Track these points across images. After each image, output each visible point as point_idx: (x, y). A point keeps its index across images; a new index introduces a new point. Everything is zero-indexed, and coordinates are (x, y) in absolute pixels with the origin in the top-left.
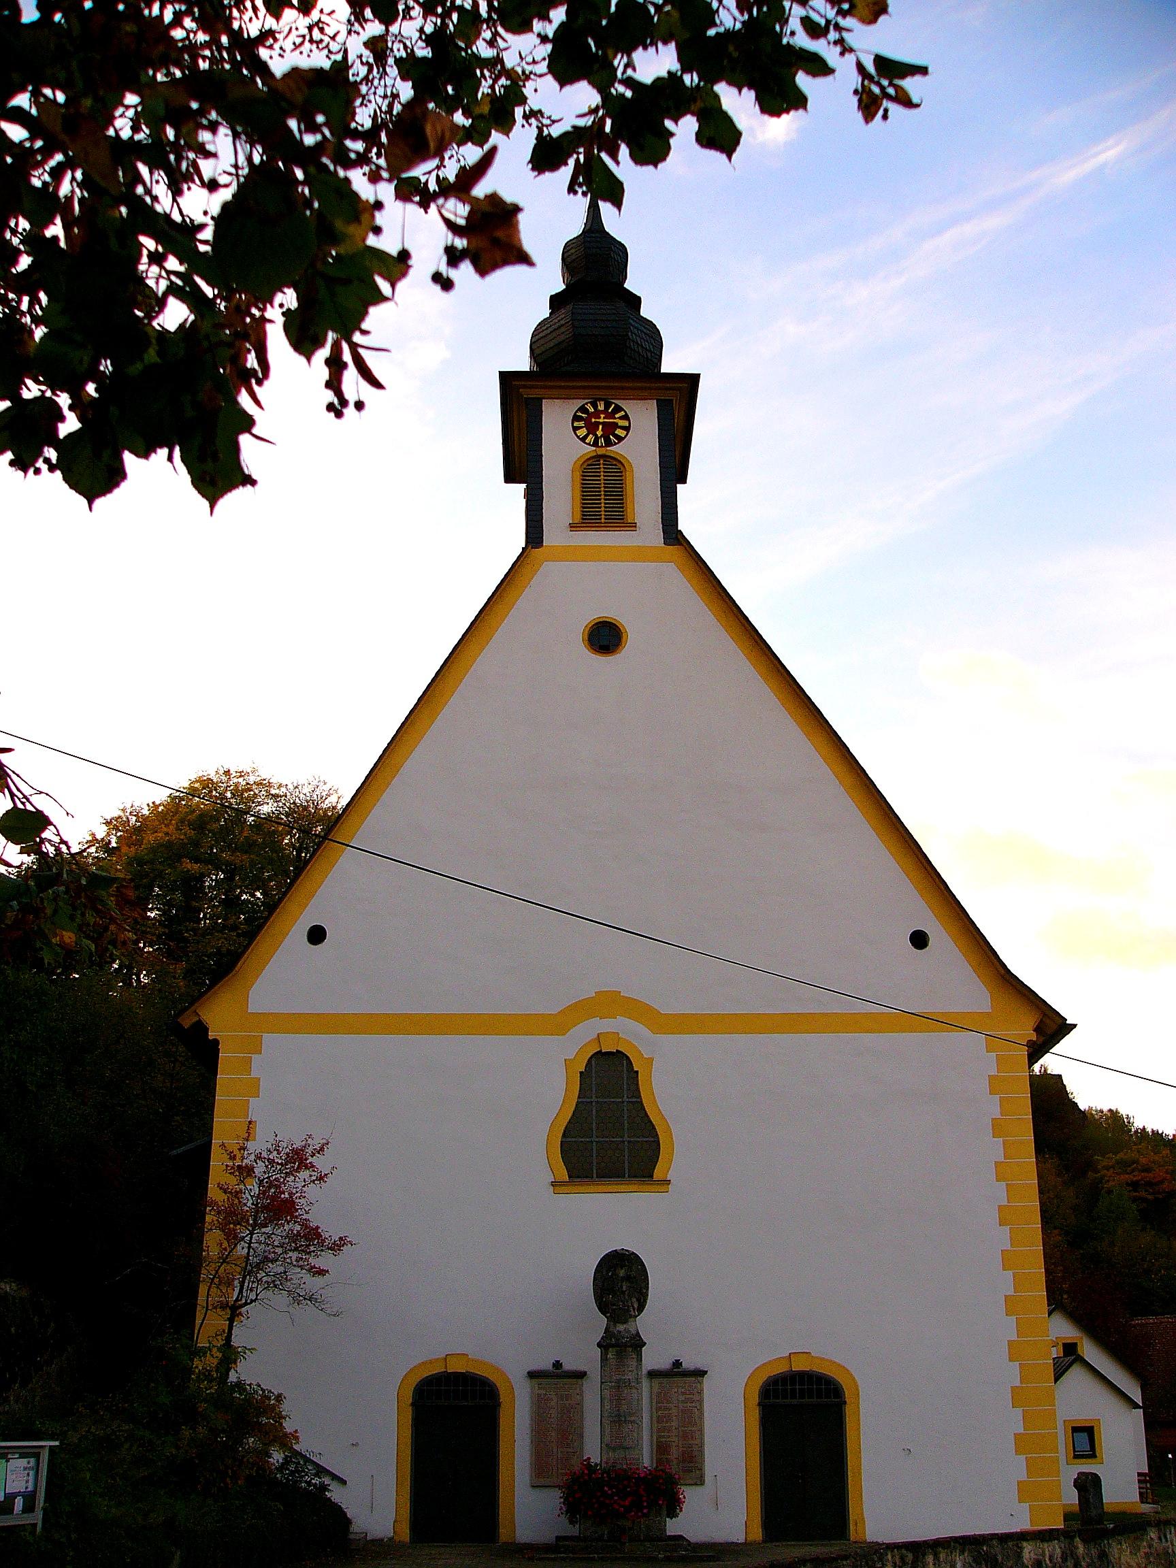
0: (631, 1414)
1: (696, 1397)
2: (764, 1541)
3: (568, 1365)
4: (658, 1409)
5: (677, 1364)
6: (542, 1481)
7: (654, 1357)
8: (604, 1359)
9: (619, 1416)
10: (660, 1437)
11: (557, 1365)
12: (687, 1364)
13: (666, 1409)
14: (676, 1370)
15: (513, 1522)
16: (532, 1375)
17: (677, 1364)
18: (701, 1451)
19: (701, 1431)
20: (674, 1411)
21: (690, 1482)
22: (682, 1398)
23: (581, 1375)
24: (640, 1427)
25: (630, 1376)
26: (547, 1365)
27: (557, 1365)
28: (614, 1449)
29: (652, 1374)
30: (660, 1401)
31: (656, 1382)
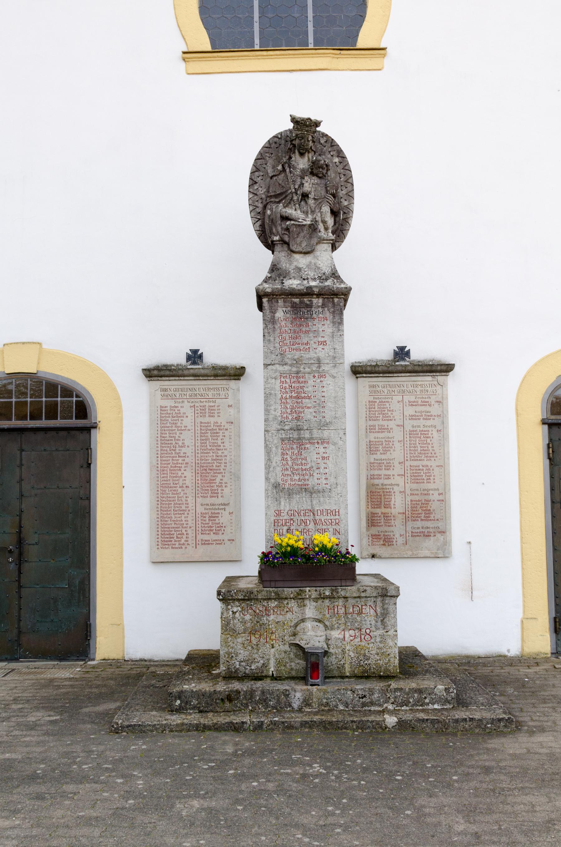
0: (323, 425)
1: (435, 410)
2: (556, 653)
3: (213, 357)
4: (371, 429)
5: (402, 353)
6: (168, 554)
7: (365, 334)
8: (270, 323)
9: (299, 429)
10: (372, 477)
11: (195, 356)
13: (382, 429)
14: (401, 364)
15: (119, 625)
16: (153, 373)
17: (402, 353)
18: (444, 501)
19: (444, 467)
20: (397, 434)
21: (426, 553)
22: (410, 411)
23: (237, 373)
24: (341, 450)
25: (322, 353)
26: (177, 357)
27: (195, 356)
28: (290, 493)
29: (358, 371)
30: (375, 412)
31: (365, 382)
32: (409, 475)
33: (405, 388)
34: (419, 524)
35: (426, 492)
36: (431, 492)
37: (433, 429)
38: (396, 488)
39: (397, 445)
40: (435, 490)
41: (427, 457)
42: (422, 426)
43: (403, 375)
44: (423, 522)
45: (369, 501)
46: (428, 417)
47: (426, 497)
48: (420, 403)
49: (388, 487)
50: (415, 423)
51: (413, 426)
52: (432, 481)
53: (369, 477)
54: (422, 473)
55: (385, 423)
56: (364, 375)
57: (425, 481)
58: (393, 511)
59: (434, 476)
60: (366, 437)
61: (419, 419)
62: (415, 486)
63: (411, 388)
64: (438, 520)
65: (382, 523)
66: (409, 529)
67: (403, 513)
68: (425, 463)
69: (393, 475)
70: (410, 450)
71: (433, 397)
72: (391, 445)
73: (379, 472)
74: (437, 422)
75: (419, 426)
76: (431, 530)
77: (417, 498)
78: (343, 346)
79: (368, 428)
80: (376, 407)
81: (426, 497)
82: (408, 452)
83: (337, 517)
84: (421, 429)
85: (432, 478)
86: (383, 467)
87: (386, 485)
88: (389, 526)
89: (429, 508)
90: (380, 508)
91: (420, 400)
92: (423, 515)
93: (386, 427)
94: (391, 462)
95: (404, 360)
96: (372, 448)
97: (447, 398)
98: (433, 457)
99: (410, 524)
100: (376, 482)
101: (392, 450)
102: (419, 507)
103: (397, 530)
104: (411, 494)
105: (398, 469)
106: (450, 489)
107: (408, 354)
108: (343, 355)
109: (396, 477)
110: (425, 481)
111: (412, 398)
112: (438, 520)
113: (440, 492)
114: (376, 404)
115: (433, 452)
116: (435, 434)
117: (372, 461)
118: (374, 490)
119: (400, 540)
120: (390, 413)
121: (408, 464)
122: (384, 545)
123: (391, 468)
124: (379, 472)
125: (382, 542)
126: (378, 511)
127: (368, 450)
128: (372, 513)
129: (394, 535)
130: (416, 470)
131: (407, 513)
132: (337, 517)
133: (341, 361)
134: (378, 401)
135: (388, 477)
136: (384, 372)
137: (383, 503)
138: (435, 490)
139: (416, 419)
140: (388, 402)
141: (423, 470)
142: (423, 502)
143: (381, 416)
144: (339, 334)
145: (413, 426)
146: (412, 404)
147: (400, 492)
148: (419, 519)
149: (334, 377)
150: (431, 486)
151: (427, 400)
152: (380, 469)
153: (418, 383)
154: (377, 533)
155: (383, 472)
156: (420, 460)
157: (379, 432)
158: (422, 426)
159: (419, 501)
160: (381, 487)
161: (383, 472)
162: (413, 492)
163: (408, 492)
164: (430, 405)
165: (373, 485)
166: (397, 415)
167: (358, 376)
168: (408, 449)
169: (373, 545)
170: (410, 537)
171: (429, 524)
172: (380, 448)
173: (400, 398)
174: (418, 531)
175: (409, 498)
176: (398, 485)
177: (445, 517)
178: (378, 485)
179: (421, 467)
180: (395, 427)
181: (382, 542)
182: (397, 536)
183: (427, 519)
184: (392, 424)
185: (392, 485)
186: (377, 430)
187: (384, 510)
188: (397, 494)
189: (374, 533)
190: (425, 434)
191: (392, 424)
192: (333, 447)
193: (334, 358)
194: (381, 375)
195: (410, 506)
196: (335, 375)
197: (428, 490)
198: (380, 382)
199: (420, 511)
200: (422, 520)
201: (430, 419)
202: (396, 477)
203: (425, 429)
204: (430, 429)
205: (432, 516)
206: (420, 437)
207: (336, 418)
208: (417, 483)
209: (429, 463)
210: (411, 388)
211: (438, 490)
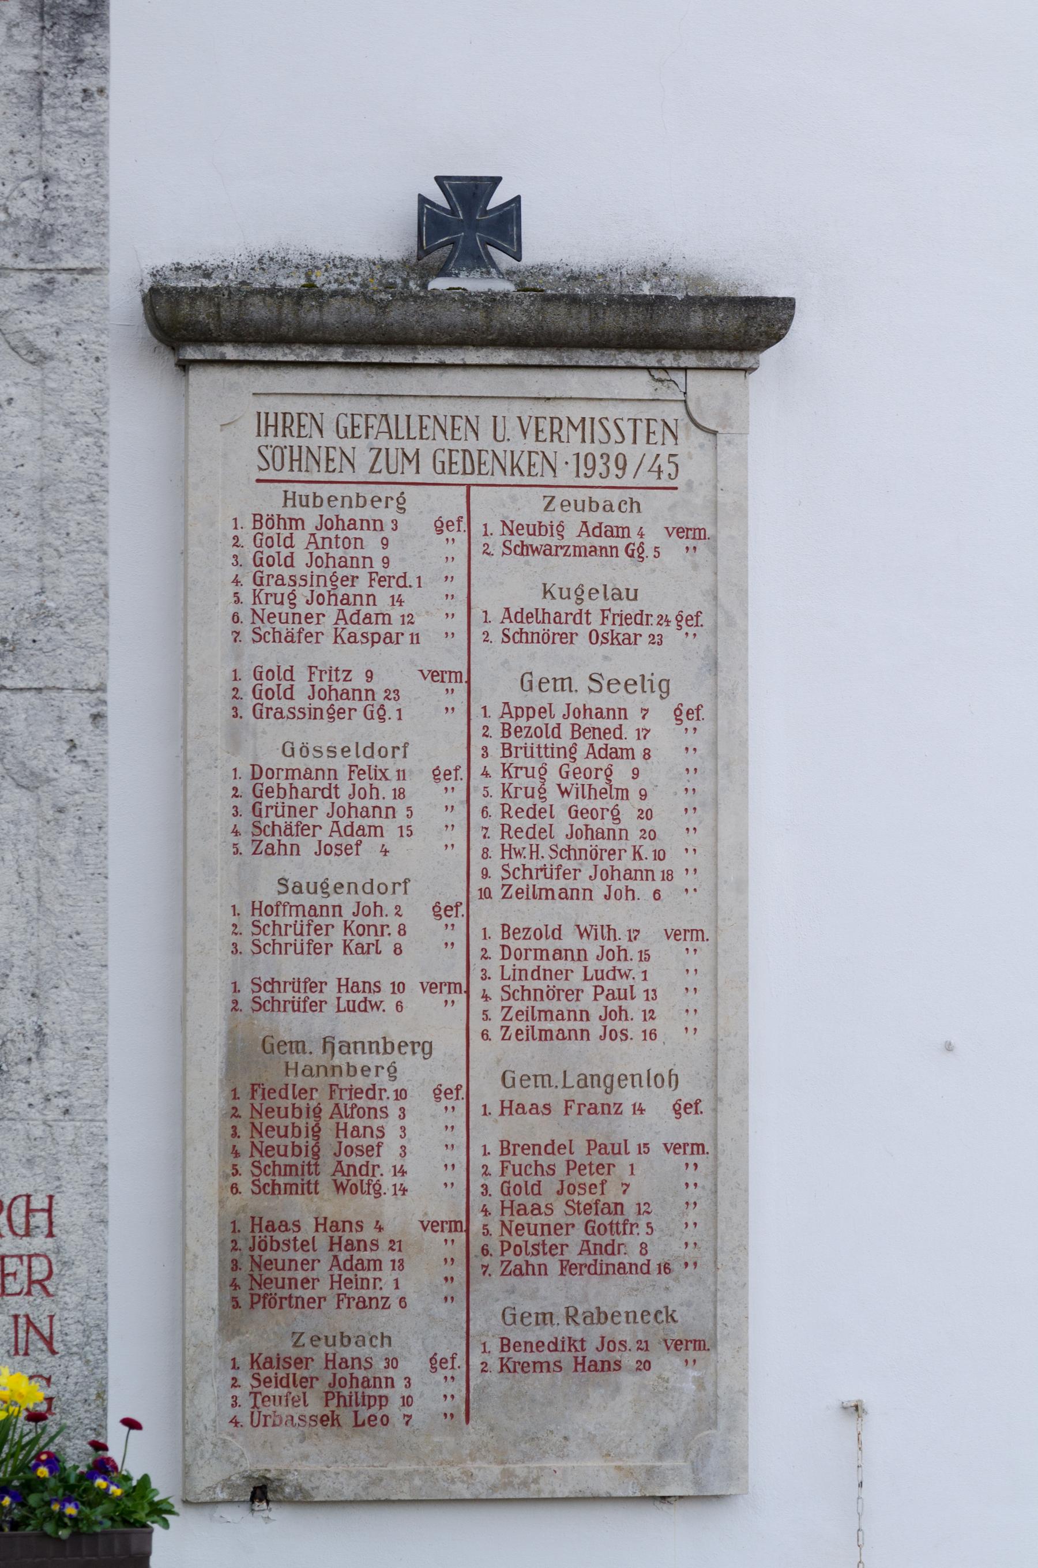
1: (664, 583)
4: (265, 694)
5: (468, 217)
10: (268, 994)
12: (574, 226)
13: (335, 697)
14: (462, 287)
17: (468, 217)
20: (428, 732)
21: (594, 1472)
22: (510, 584)
29: (193, 323)
30: (301, 581)
31: (233, 398)
32: (494, 987)
33: (486, 440)
34: (551, 1291)
35: (596, 1095)
36: (628, 1096)
37: (653, 700)
38: (408, 1064)
39: (427, 799)
40: (654, 1080)
41: (607, 875)
42: (581, 682)
43: (472, 356)
44: (577, 1283)
45: (244, 1144)
46: (623, 627)
47: (600, 1128)
48: (571, 537)
49: (359, 1060)
50: (544, 660)
51: (526, 682)
52: (635, 1027)
53: (246, 995)
54: (576, 980)
55: (354, 658)
56: (231, 352)
57: (595, 1028)
58: (390, 1208)
59: (651, 995)
60: (235, 742)
61: (568, 638)
62: (529, 1056)
63: (521, 445)
64: (665, 1268)
65: (323, 1288)
66: (487, 1322)
67: (454, 1226)
68: (596, 912)
69: (398, 987)
70: (505, 831)
71: (655, 503)
72: (387, 798)
73: (312, 967)
74: (674, 657)
75: (565, 684)
76: (624, 1332)
77: (540, 1130)
78: (100, 161)
79: (247, 685)
80: (301, 557)
81: (600, 1128)
82: (495, 844)
83: (39, 1243)
84: (578, 700)
85: (635, 1007)
86: (337, 936)
87: (347, 1047)
88: (363, 1304)
89: (612, 1195)
90: (310, 1189)
91: (573, 521)
92: (577, 1236)
93: (358, 681)
94: (387, 902)
95: (482, 263)
96: (267, 814)
97: (741, 511)
98: (648, 874)
99: (494, 1293)
100: (290, 1025)
101: (390, 827)
102: (551, 1185)
103: (415, 1328)
104: (508, 1108)
105: (427, 951)
106: (743, 1080)
107: (507, 224)
108: (100, 218)
109: (415, 999)
110: (595, 1028)
111: (528, 507)
112: (665, 1268)
113: (686, 1093)
114: (301, 538)
115: (647, 848)
116: (664, 735)
117: (268, 894)
118: (274, 1078)
119: (432, 1395)
120: (383, 596)
121: (489, 915)
122: (329, 1420)
123: (386, 944)
124: (312, 967)
125: (315, 1407)
126: (298, 1208)
127: (245, 823)
128: (255, 1222)
129: (392, 1363)
130: (542, 954)
131: (477, 1221)
132: (39, 1243)
133: (88, 257)
134: (311, 516)
135: (363, 998)
136: (354, 338)
137: (327, 1163)
138: (654, 1080)
139: (545, 638)
140: (376, 525)
141: (581, 955)
142: (580, 1156)
143: (331, 612)
144: (77, 83)
145: (526, 682)
146: (523, 542)
147: (439, 1093)
148: (554, 1265)
149: (40, 358)
150: (629, 1057)
151: (615, 519)
152: (316, 949)
153: (564, 411)
154: (288, 1349)
155: (335, 966)
156: (565, 895)
157: (314, 714)
158: (581, 682)
159: (553, 1148)
160: (317, 1057)
161: (335, 966)
162: (517, 1095)
163: (487, 1091)
164: (636, 553)
165: (270, 1046)
166: (431, 609)
167: (191, 353)
168: (495, 822)
169: (260, 1420)
170: (493, 1376)
171: (613, 1293)
172: (320, 817)
173: (451, 502)
174: (546, 1334)
175: (490, 1133)
176: (426, 1049)
177: (712, 1254)
178: (298, 1046)
179: (570, 941)
180: (413, 686)
181: (315, 1407)
182: (414, 1365)
183: (601, 1260)
184: (393, 666)
185: (387, 1046)
186: (301, 700)
187: (334, 1206)
188: (420, 1102)
189: (267, 1348)
190: (601, 732)
191: (393, 666)
192: (25, 801)
193: (45, 234)
194: (337, 354)
195: (495, 1184)
196: (44, 343)
197: (611, 1082)
198: (326, 395)
199: (559, 1216)
200: (567, 1268)
201: (631, 640)
202: (415, 999)
203: (604, 700)
204: (633, 702)
205: (631, 1242)
206: (571, 753)
207: (43, 615)
208: (546, 1035)
209: (618, 915)
210: (521, 445)
211: (673, 1080)
